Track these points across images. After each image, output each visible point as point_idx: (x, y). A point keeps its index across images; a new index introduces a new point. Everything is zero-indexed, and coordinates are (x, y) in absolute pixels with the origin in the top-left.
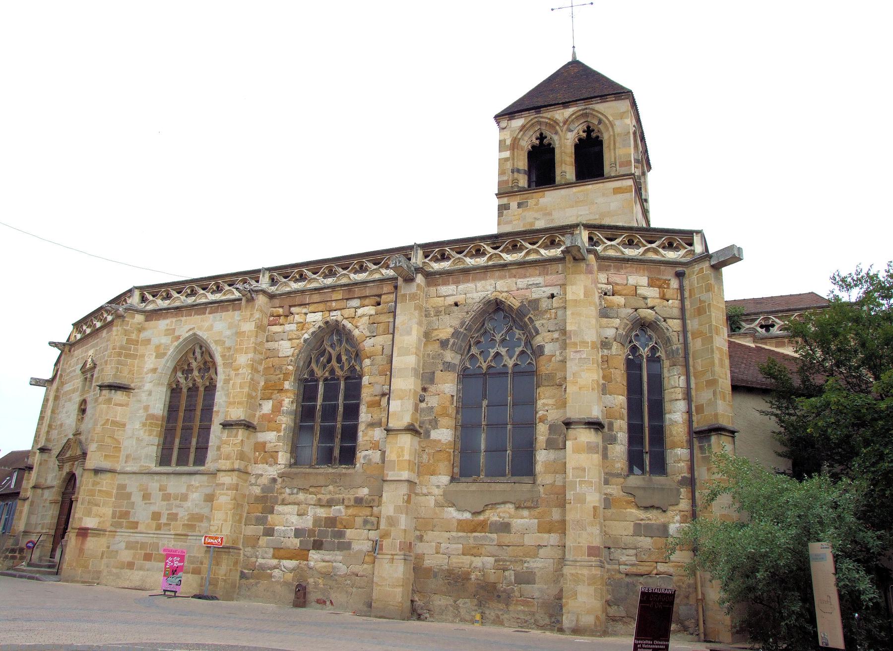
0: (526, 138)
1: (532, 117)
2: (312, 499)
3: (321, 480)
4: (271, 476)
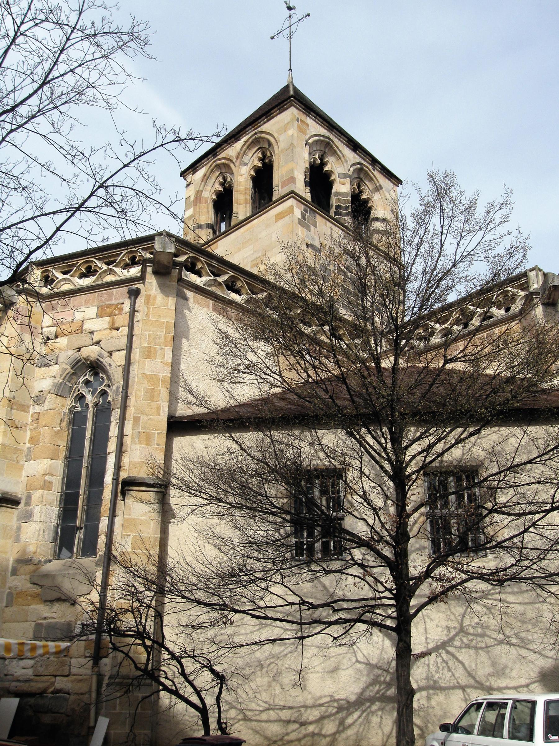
0: (209, 188)
1: (211, 163)
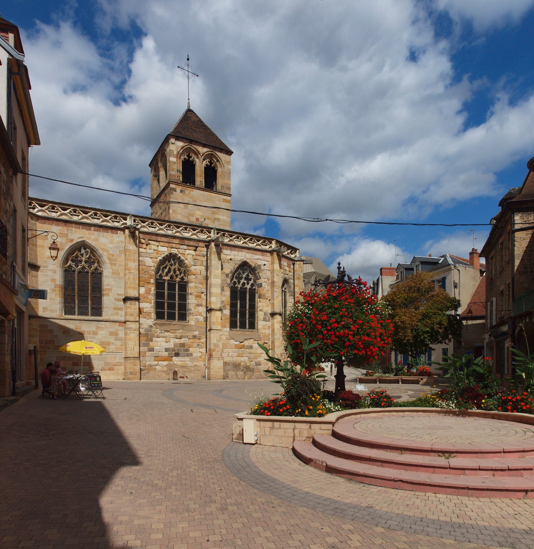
2: (172, 335)
3: (176, 327)
4: (149, 325)
